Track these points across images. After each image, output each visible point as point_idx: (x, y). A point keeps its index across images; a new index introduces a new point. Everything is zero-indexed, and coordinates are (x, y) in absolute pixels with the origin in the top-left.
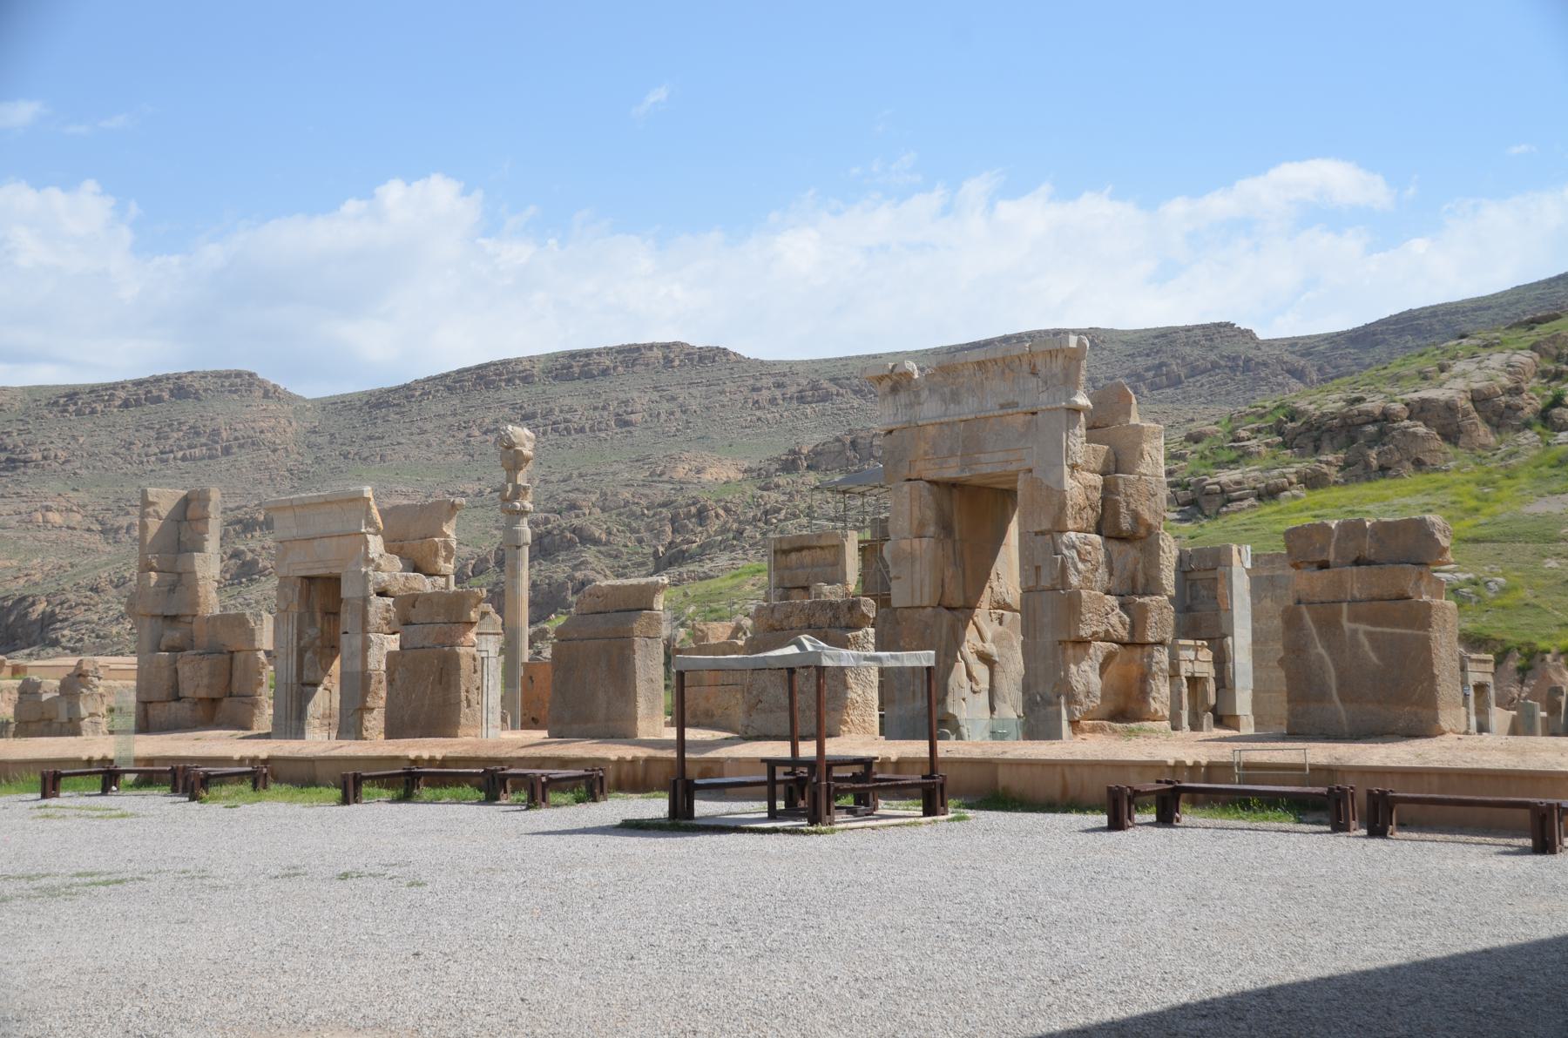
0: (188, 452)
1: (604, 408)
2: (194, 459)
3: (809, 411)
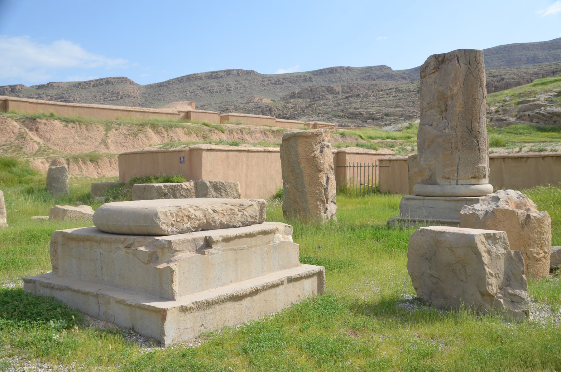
0: (111, 98)
1: (223, 86)
2: (113, 100)
3: (278, 87)
